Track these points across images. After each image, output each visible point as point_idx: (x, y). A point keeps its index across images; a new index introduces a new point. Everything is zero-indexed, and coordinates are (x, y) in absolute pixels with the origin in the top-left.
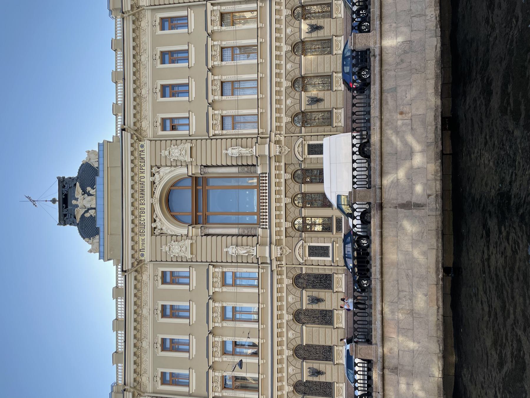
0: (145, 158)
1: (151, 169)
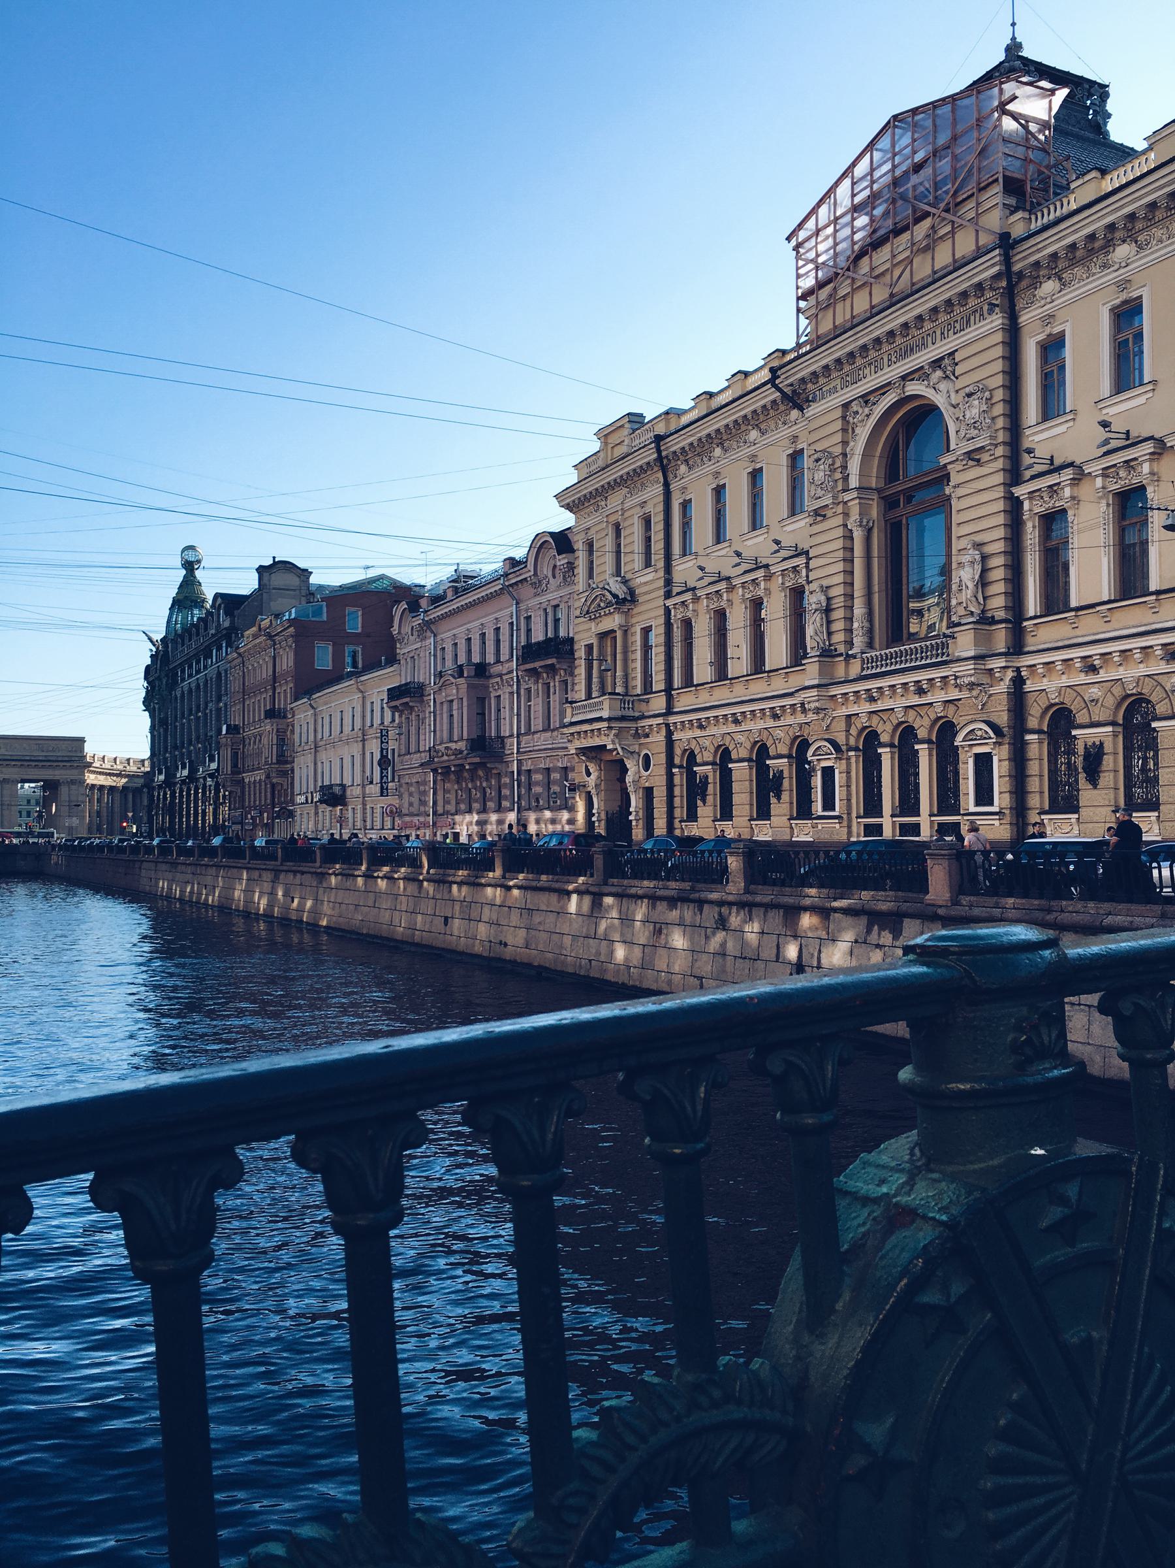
0: (969, 330)
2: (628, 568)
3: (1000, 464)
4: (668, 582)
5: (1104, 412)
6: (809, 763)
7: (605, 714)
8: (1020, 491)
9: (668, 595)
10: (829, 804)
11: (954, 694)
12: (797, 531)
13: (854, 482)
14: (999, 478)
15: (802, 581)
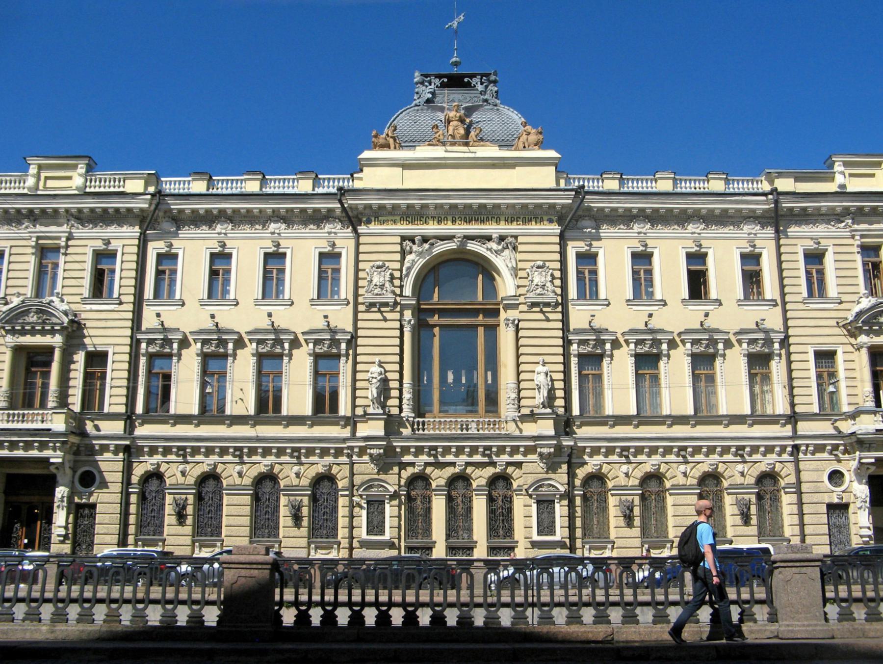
1: (512, 236)
11: (518, 458)
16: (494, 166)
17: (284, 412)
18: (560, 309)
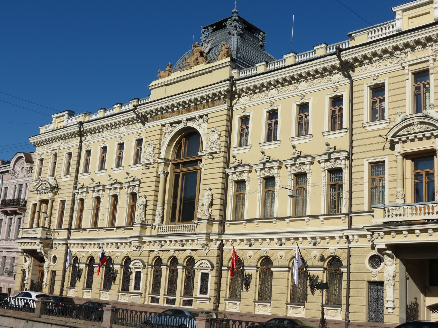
2: (58, 173)
3: (222, 159)
4: (76, 183)
5: (262, 147)
6: (130, 268)
7: (39, 236)
8: (229, 171)
9: (75, 188)
10: (137, 287)
12: (137, 171)
13: (163, 155)
14: (221, 165)
15: (137, 192)
16: (203, 74)
17: (116, 226)
18: (222, 154)
